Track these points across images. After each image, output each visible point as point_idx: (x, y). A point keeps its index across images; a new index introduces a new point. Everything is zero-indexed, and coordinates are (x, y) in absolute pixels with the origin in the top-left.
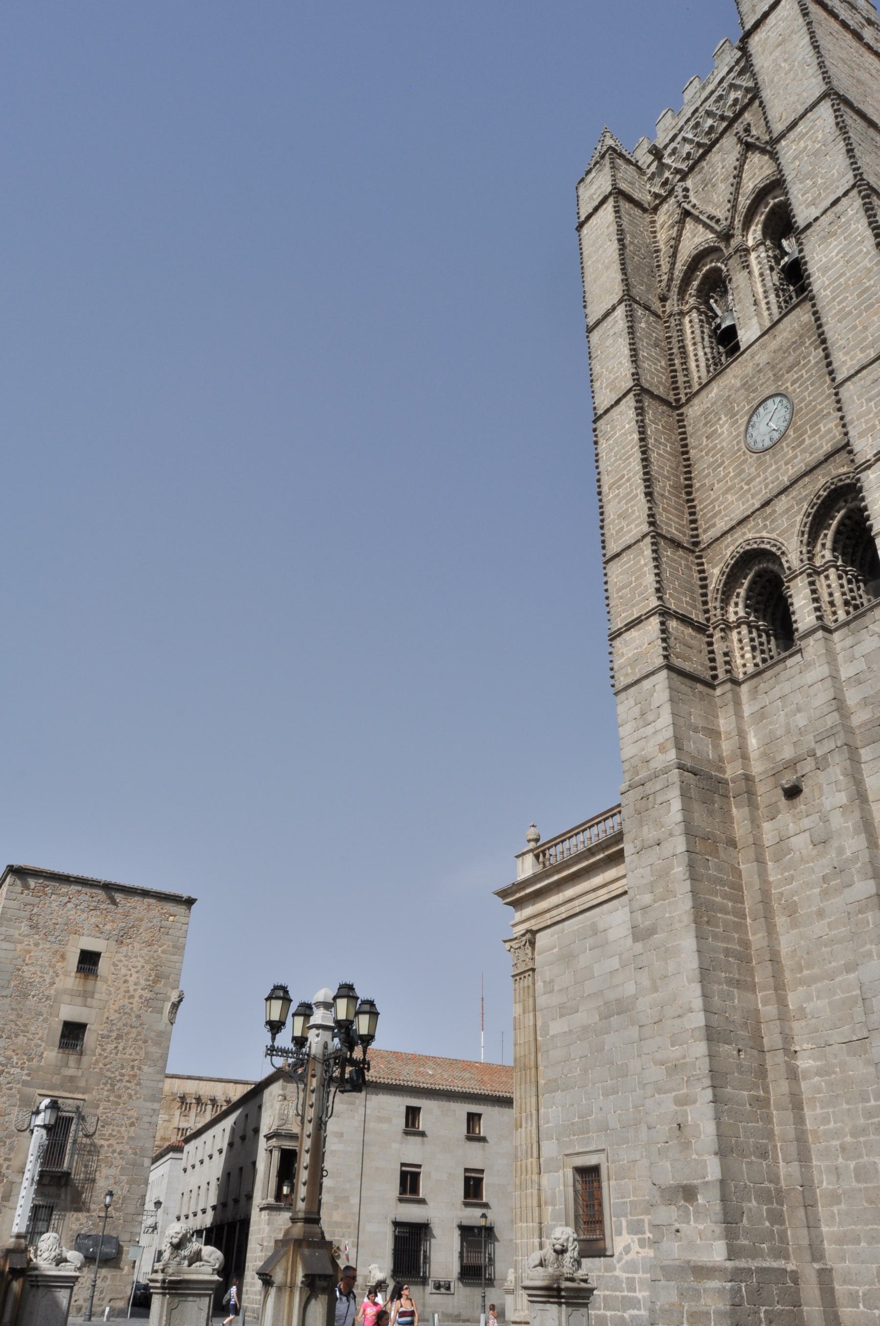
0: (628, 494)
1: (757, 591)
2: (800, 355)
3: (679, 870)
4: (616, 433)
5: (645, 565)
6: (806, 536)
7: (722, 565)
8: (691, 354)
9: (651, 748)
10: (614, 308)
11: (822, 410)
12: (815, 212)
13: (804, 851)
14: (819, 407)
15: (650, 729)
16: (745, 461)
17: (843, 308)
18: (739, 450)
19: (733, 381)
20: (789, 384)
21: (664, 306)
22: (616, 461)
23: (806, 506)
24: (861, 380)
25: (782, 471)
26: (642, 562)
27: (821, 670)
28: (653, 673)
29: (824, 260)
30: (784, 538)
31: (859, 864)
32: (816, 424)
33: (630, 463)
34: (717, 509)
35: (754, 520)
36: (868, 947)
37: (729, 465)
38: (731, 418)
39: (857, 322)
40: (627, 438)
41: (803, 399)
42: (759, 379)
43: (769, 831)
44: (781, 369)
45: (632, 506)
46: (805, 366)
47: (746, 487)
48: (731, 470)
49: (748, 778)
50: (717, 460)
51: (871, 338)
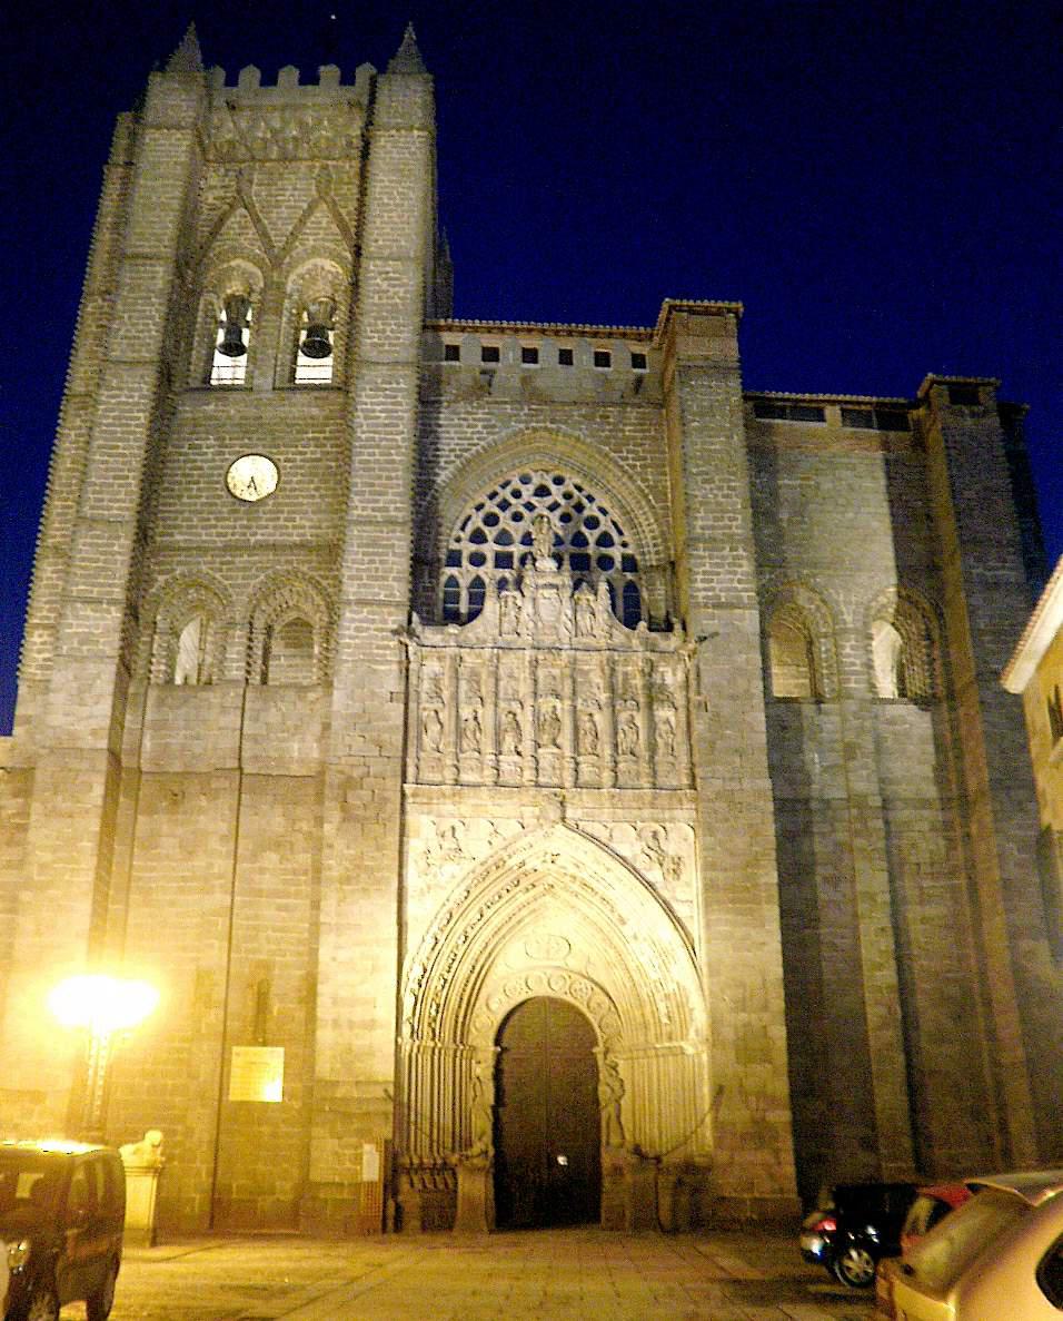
5: (120, 553)
9: (80, 727)
11: (302, 504)
12: (373, 355)
14: (301, 500)
15: (85, 711)
16: (220, 497)
17: (369, 461)
18: (217, 482)
23: (262, 577)
26: (116, 548)
32: (294, 512)
33: (128, 440)
34: (179, 522)
38: (220, 446)
41: (291, 482)
45: (120, 486)
46: (301, 453)
47: (213, 522)
50: (192, 475)
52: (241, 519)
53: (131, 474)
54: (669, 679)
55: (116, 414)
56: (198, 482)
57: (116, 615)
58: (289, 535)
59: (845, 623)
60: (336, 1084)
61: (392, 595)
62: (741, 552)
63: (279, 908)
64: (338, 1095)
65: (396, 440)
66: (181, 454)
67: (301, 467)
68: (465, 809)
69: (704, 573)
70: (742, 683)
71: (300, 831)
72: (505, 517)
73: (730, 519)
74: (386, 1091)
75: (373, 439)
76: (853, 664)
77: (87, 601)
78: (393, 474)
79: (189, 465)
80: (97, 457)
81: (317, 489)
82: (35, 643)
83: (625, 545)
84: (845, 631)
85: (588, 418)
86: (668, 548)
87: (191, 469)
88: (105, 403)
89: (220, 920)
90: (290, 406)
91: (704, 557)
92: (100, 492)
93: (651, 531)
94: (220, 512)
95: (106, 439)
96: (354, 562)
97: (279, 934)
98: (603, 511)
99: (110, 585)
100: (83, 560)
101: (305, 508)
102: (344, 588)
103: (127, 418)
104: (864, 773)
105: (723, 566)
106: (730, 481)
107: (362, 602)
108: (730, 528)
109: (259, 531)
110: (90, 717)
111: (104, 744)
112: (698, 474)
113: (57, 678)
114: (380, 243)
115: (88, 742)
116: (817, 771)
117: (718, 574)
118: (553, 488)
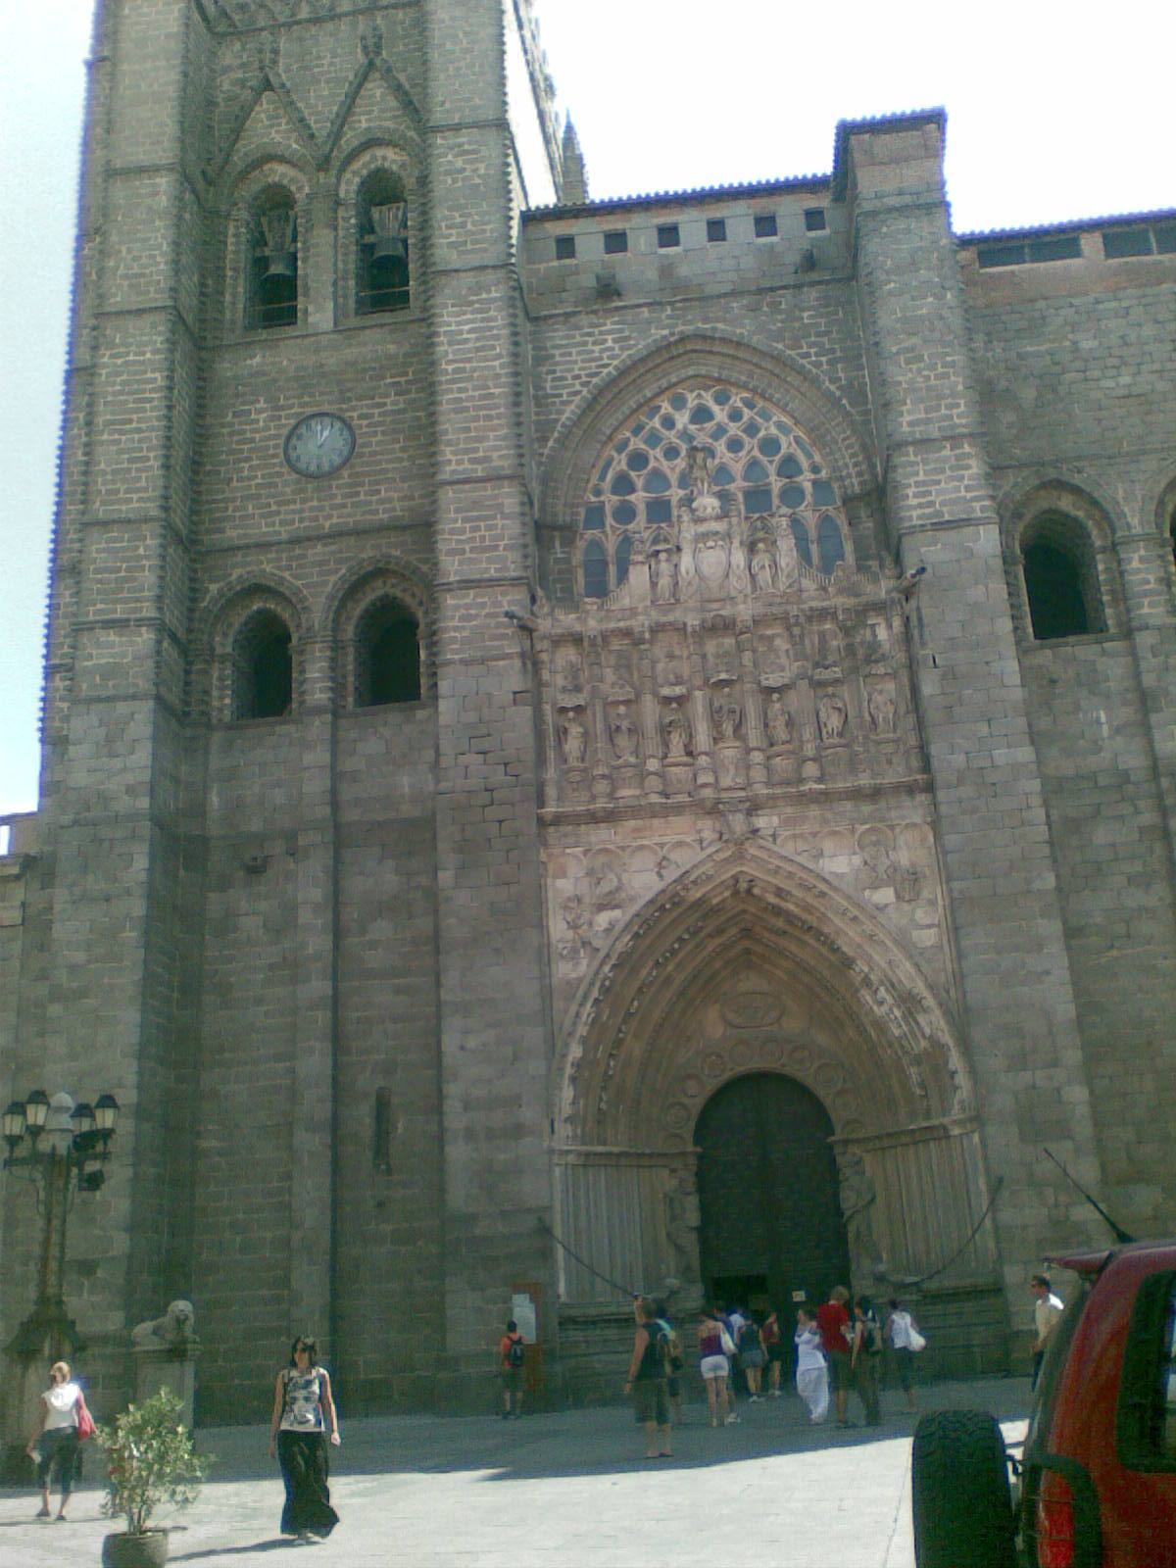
0: (133, 450)
3: (131, 935)
4: (128, 354)
5: (146, 557)
6: (336, 603)
7: (222, 584)
8: (228, 281)
10: (154, 170)
11: (386, 471)
15: (117, 763)
16: (282, 474)
18: (274, 456)
20: (355, 414)
21: (208, 191)
22: (121, 393)
23: (343, 571)
24: (462, 491)
26: (141, 551)
27: (319, 756)
28: (134, 697)
29: (453, 328)
32: (378, 483)
33: (144, 410)
34: (230, 513)
39: (472, 425)
40: (146, 372)
41: (369, 444)
43: (215, 902)
44: (350, 390)
47: (274, 508)
49: (205, 840)
50: (241, 451)
51: (481, 454)
52: (312, 500)
53: (152, 455)
54: (882, 634)
55: (125, 377)
56: (248, 459)
57: (146, 637)
58: (371, 512)
60: (473, 1218)
61: (507, 569)
62: (967, 448)
63: (398, 991)
64: (478, 1231)
65: (494, 367)
66: (223, 426)
67: (381, 423)
69: (918, 484)
72: (656, 457)
73: (949, 407)
74: (540, 1219)
75: (463, 370)
77: (109, 624)
78: (493, 412)
79: (235, 438)
80: (105, 437)
81: (403, 450)
82: (57, 690)
83: (815, 469)
84: (1130, 540)
85: (754, 309)
86: (872, 466)
87: (237, 442)
88: (105, 365)
89: (320, 1014)
91: (917, 464)
92: (113, 482)
93: (848, 447)
95: (113, 413)
96: (452, 532)
99: (137, 600)
100: (97, 571)
102: (442, 565)
103: (138, 381)
105: (942, 471)
106: (947, 354)
107: (467, 584)
108: (951, 417)
110: (125, 769)
111: (144, 803)
112: (897, 353)
113: (77, 726)
114: (447, 106)
115: (123, 804)
117: (938, 482)
118: (716, 409)
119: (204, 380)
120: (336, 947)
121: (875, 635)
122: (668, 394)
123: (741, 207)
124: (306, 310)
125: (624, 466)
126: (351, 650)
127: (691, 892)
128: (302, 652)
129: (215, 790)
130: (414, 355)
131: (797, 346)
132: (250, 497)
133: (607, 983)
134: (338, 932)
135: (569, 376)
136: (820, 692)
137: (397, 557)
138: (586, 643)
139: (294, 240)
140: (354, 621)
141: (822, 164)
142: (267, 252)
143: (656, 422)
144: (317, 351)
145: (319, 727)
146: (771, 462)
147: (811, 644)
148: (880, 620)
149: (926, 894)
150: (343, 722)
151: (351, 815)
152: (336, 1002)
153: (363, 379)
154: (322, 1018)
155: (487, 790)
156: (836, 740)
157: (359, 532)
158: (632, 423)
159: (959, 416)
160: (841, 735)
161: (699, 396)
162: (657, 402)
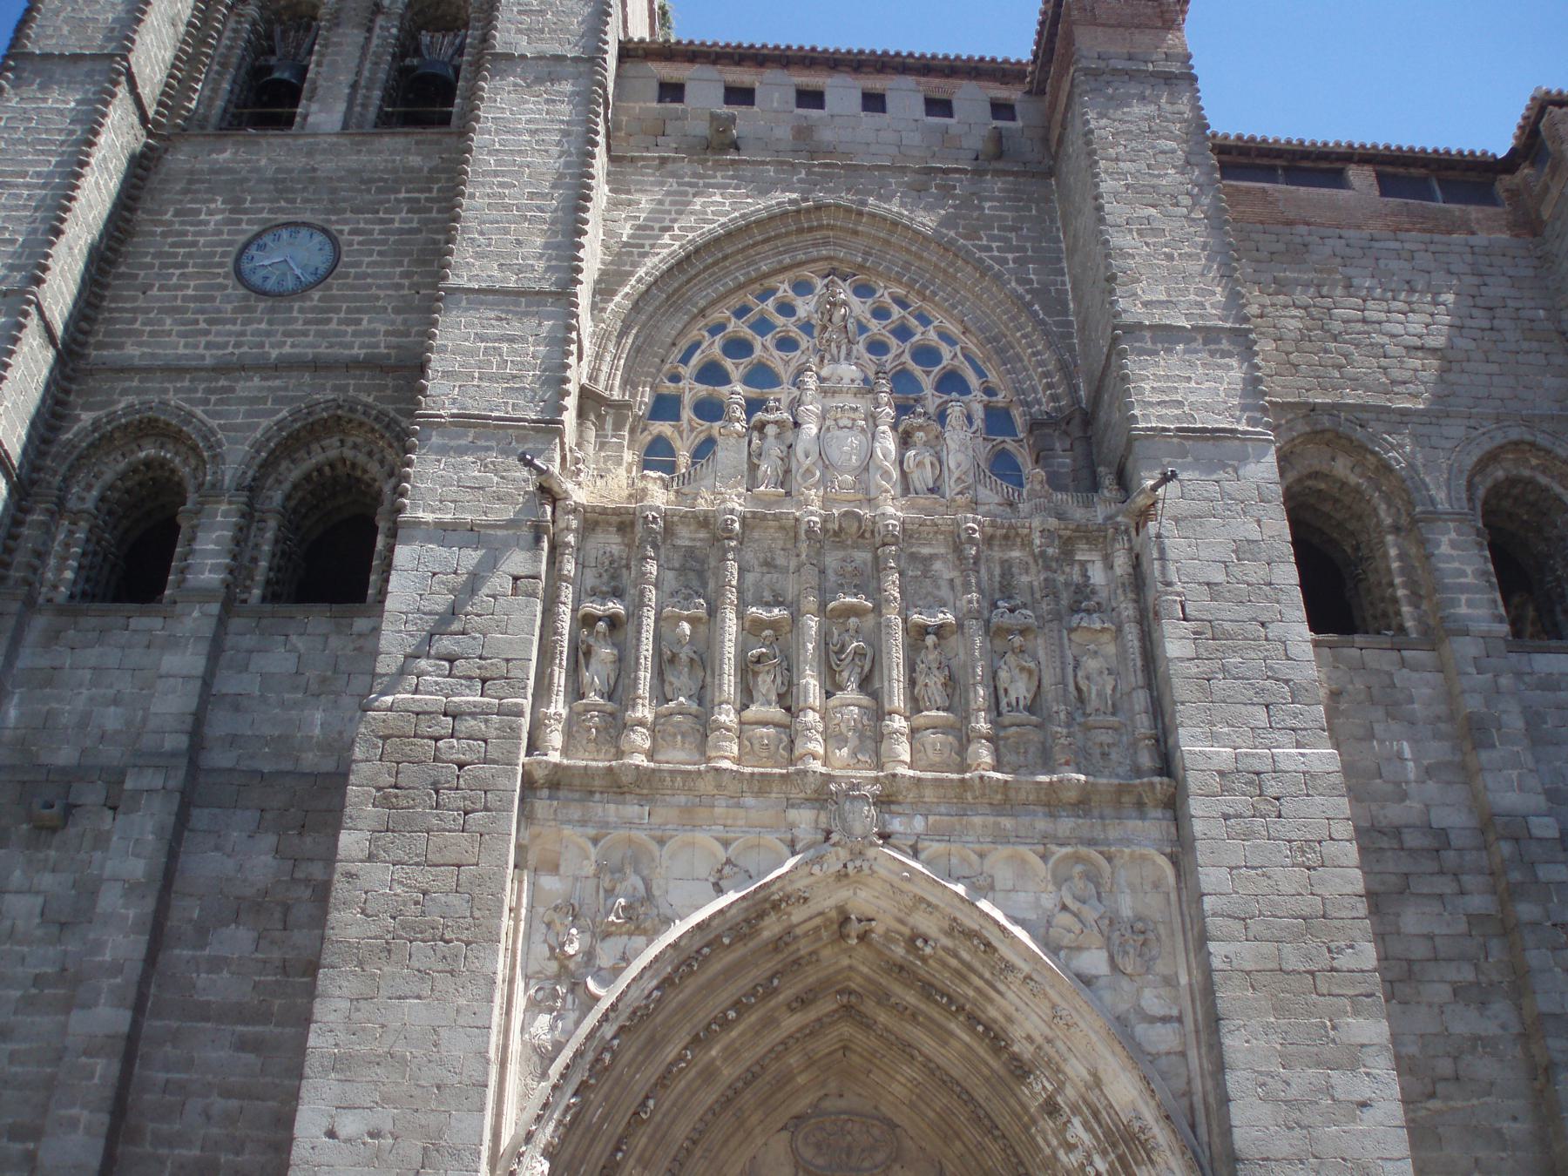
1: (129, 484)
2: (381, 202)
6: (263, 454)
11: (377, 298)
13: (20, 923)
14: (374, 291)
16: (225, 287)
18: (221, 265)
19: (263, 162)
20: (346, 228)
23: (284, 413)
25: (273, 339)
27: (188, 661)
30: (227, 438)
31: (119, 980)
32: (359, 310)
34: (137, 326)
35: (191, 381)
36: (74, 1111)
37: (198, 275)
38: (232, 211)
41: (357, 264)
42: (305, 189)
44: (344, 200)
46: (382, 222)
47: (203, 325)
48: (192, 284)
50: (175, 255)
52: (260, 321)
54: (1097, 575)
58: (341, 345)
59: (1432, 501)
62: (1225, 345)
63: (242, 1045)
67: (385, 242)
68: (663, 814)
69: (1157, 378)
70: (1255, 571)
71: (307, 881)
76: (1463, 574)
79: (170, 240)
83: (989, 391)
87: (173, 245)
90: (369, 152)
93: (1041, 364)
94: (219, 311)
97: (234, 1103)
98: (945, 336)
101: (380, 303)
104: (1514, 774)
109: (289, 341)
116: (1412, 776)
119: (147, 169)
120: (151, 959)
121: (1085, 575)
122: (791, 274)
123: (909, 81)
124: (305, 117)
125: (716, 350)
126: (272, 523)
127: (767, 921)
128: (198, 513)
129: (16, 699)
130: (444, 171)
131: (972, 235)
132: (176, 310)
133: (607, 1057)
134: (158, 934)
135: (657, 226)
136: (999, 644)
137: (366, 405)
138: (639, 528)
139: (310, 52)
140: (287, 486)
141: (1019, 46)
142: (273, 60)
143: (770, 304)
144: (310, 154)
145: (197, 620)
146: (928, 373)
147: (990, 574)
148: (1096, 557)
149: (1161, 967)
150: (236, 623)
151: (219, 758)
152: (130, 1049)
153: (368, 191)
154: (104, 1069)
155: (445, 715)
156: (1024, 716)
157: (317, 366)
158: (735, 301)
159: (1213, 306)
160: (1030, 709)
161: (832, 281)
162: (771, 282)
